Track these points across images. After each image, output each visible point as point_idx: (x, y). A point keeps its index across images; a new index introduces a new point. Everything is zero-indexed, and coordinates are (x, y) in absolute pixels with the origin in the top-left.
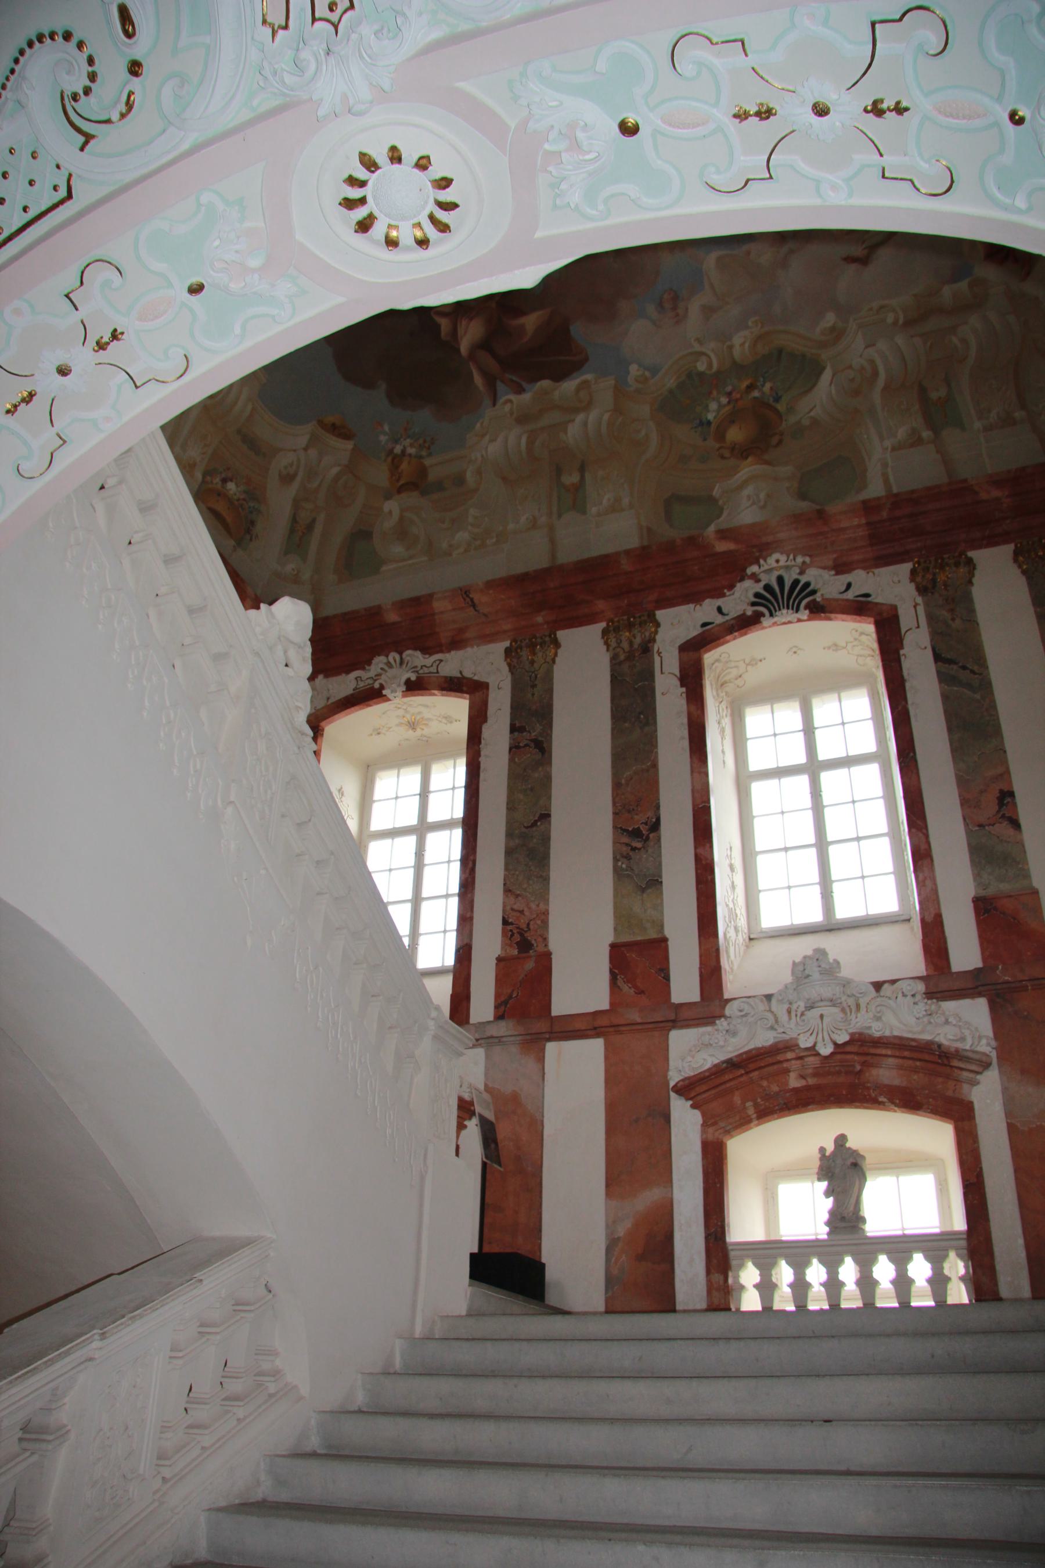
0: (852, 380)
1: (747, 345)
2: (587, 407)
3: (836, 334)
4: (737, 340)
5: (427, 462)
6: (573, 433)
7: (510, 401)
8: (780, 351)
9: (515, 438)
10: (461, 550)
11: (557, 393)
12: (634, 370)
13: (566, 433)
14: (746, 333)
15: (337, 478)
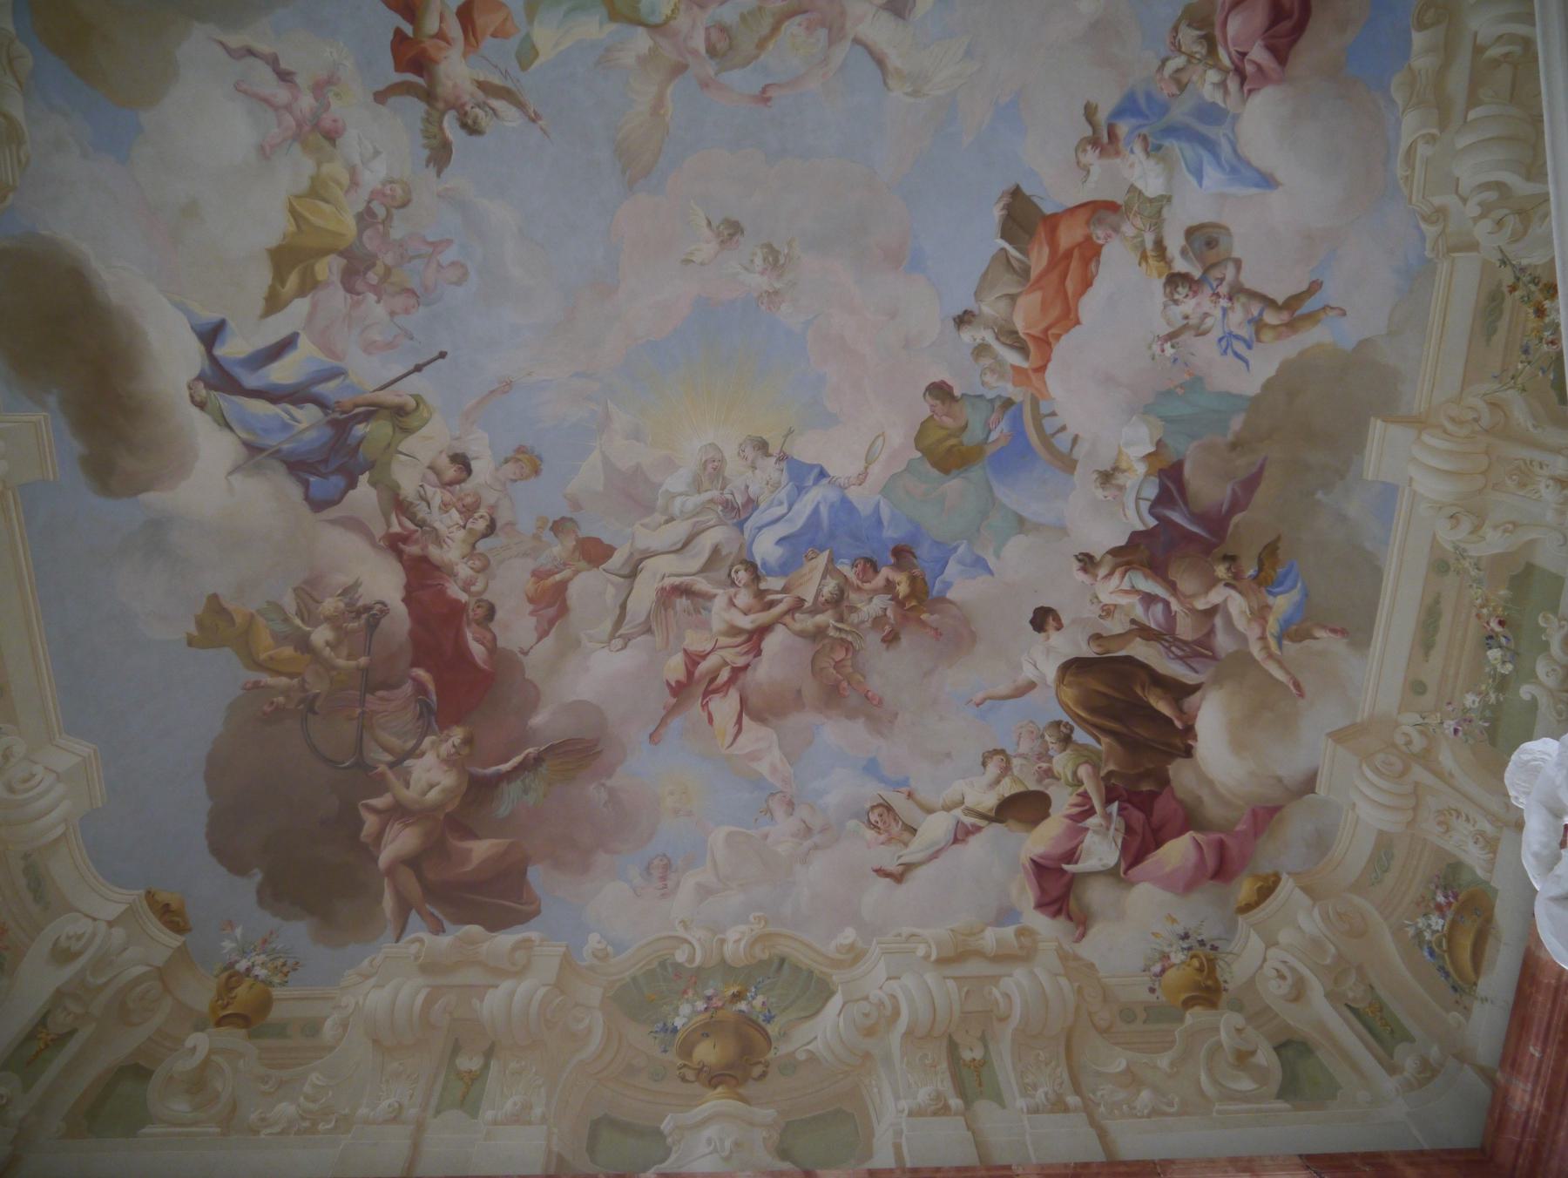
0: (866, 1015)
1: (743, 943)
2: (519, 973)
3: (855, 955)
4: (732, 935)
5: (276, 993)
7: (421, 941)
8: (783, 960)
9: (409, 991)
10: (277, 1129)
12: (594, 940)
13: (482, 1001)
14: (743, 928)
15: (138, 981)
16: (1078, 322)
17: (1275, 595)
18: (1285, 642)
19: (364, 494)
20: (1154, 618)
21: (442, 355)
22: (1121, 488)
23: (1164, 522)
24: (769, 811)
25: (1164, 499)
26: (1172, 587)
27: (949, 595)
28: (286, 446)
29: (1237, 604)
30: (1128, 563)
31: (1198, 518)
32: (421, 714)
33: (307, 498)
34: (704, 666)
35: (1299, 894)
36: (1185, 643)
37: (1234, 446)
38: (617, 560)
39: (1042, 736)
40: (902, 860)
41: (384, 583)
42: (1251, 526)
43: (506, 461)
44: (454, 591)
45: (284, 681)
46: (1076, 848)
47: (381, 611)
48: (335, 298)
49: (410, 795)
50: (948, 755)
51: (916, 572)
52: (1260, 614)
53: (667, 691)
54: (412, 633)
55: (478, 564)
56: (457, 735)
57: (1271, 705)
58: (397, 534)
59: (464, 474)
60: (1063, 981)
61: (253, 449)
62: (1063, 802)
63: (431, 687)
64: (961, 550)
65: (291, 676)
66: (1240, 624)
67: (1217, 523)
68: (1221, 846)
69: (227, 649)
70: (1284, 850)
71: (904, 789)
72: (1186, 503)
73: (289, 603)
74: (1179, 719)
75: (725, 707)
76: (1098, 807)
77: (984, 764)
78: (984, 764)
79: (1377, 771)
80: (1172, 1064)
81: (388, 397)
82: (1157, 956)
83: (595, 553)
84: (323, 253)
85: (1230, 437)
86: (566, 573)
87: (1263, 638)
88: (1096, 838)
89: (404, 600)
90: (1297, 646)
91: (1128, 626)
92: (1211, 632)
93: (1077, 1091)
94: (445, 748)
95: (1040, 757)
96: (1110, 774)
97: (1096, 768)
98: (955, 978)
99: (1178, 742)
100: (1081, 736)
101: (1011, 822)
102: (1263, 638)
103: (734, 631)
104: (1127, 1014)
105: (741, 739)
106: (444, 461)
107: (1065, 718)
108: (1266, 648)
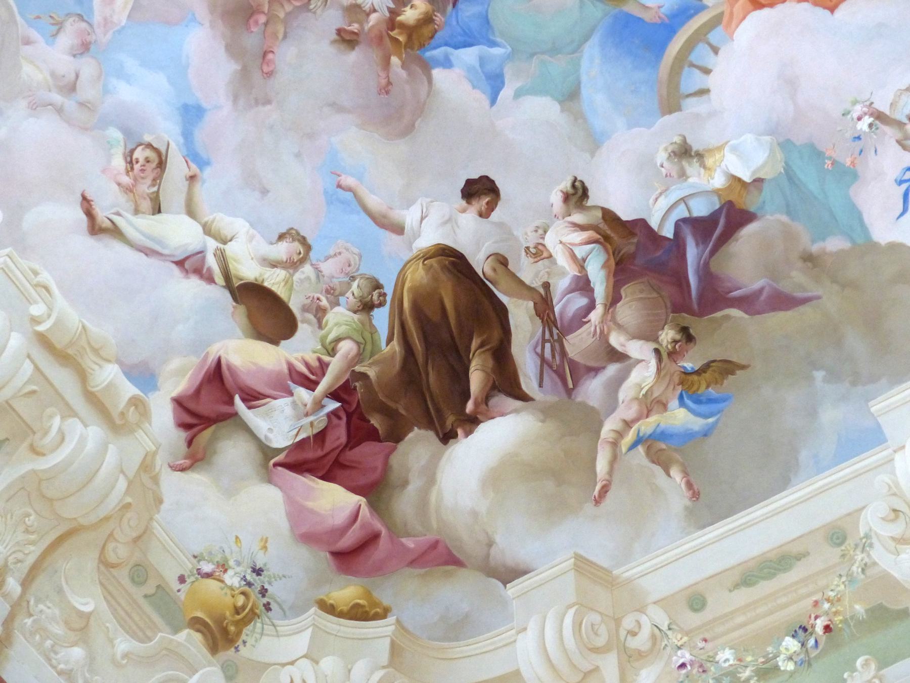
16: (832, 10)
17: (682, 404)
18: (641, 449)
20: (566, 304)
22: (683, 175)
23: (678, 242)
24: (59, 26)
25: (702, 227)
26: (614, 299)
27: (437, 73)
29: (644, 375)
30: (607, 238)
31: (707, 276)
35: (384, 646)
36: (563, 353)
37: (809, 259)
39: (353, 278)
40: (116, 219)
42: (734, 332)
46: (266, 396)
50: (265, 192)
51: (439, 18)
52: (651, 404)
57: (565, 478)
60: (122, 484)
62: (301, 348)
64: (496, 51)
66: (626, 392)
67: (715, 296)
68: (372, 539)
70: (416, 599)
71: (194, 168)
72: (713, 252)
74: (476, 404)
76: (321, 388)
77: (281, 237)
78: (281, 237)
79: (577, 625)
80: (125, 655)
82: (218, 558)
85: (815, 248)
87: (628, 424)
88: (289, 411)
90: (645, 462)
91: (537, 284)
92: (595, 371)
93: (26, 583)
95: (329, 291)
96: (364, 376)
97: (359, 357)
98: (37, 368)
99: (450, 420)
100: (381, 318)
101: (242, 309)
102: (628, 424)
104: (140, 573)
107: (389, 290)
108: (620, 434)
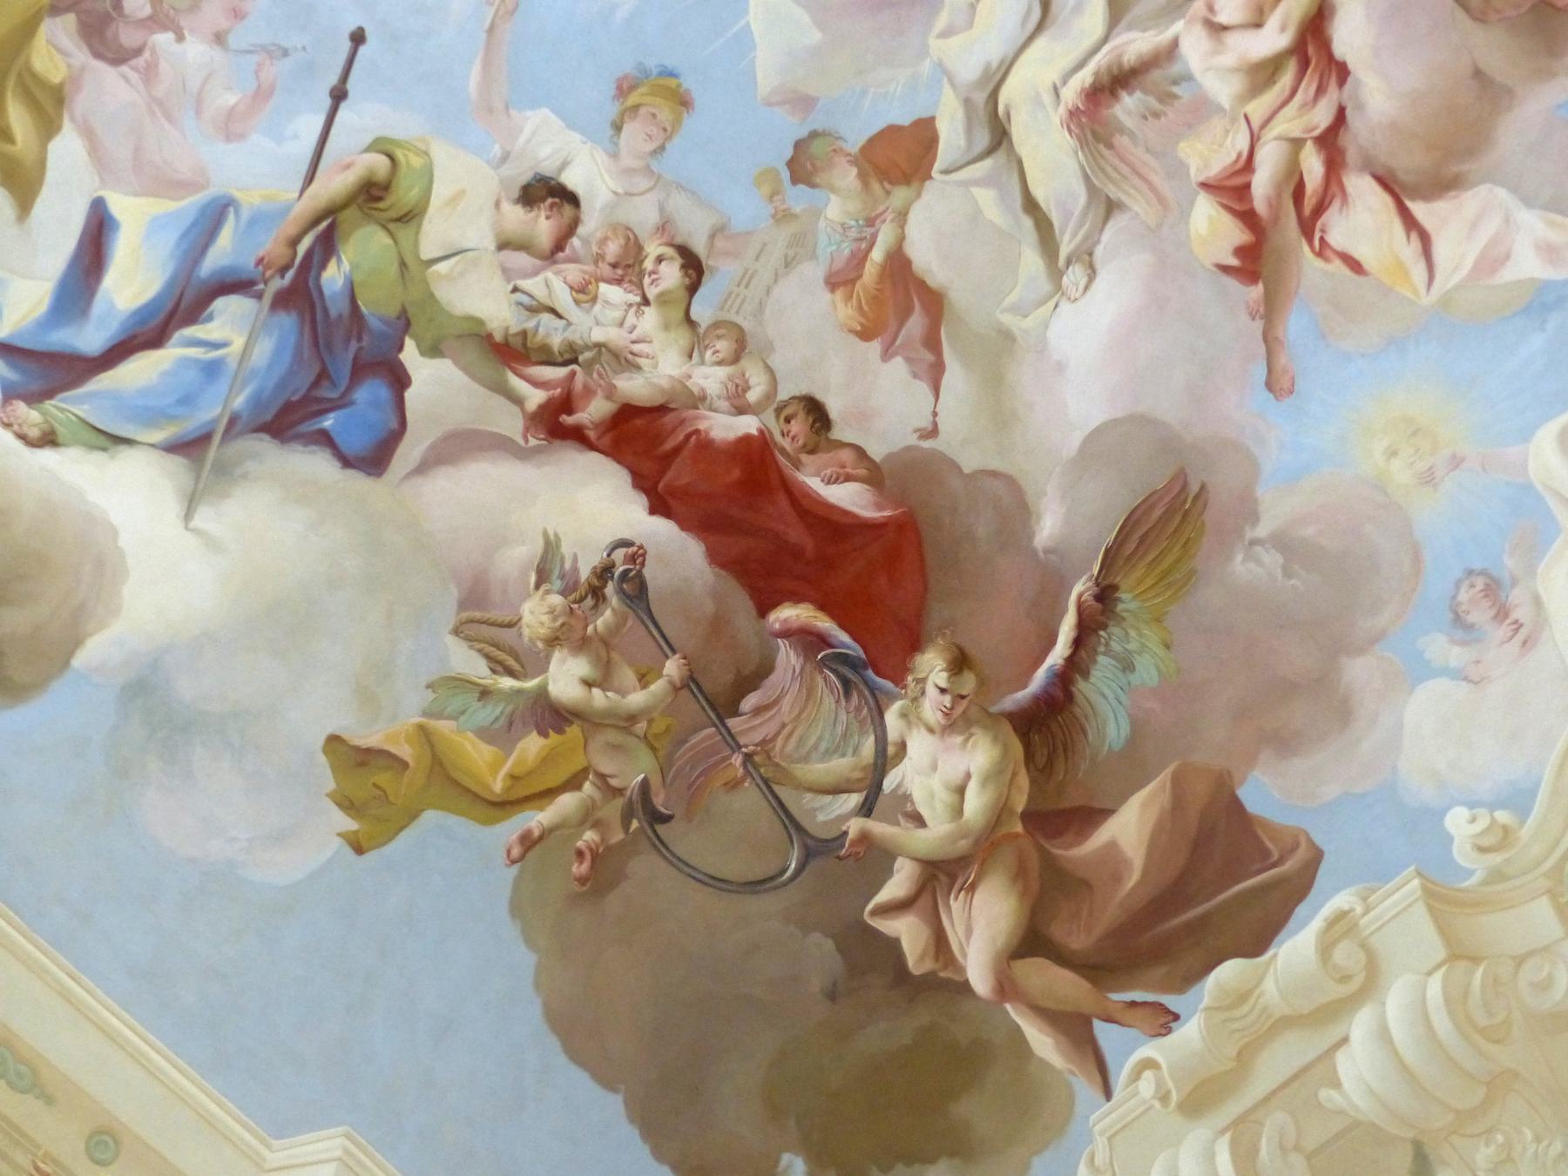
2: (1369, 985)
6: (1359, 1072)
7: (1150, 1064)
11: (1269, 985)
12: (1458, 823)
13: (1336, 1084)
19: (434, 382)
21: (358, 38)
28: (239, 402)
32: (847, 685)
33: (347, 462)
34: (1262, 183)
38: (952, 135)
41: (597, 507)
43: (618, 127)
44: (725, 427)
45: (567, 802)
47: (632, 559)
48: (107, 91)
49: (936, 834)
53: (1232, 283)
54: (714, 557)
55: (724, 346)
56: (932, 666)
58: (543, 408)
59: (568, 210)
61: (190, 447)
63: (825, 624)
65: (573, 783)
69: (430, 817)
73: (469, 663)
75: (1362, 220)
81: (334, 184)
83: (903, 156)
84: (28, 29)
86: (885, 238)
89: (653, 511)
94: (932, 707)
103: (1262, 74)
105: (1440, 250)
106: (515, 216)
